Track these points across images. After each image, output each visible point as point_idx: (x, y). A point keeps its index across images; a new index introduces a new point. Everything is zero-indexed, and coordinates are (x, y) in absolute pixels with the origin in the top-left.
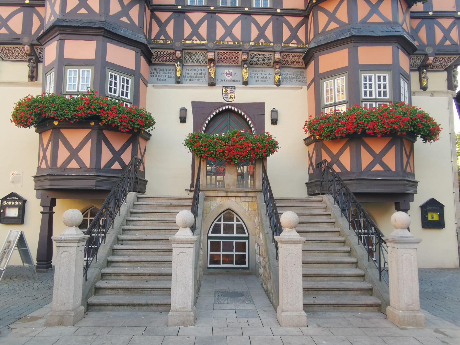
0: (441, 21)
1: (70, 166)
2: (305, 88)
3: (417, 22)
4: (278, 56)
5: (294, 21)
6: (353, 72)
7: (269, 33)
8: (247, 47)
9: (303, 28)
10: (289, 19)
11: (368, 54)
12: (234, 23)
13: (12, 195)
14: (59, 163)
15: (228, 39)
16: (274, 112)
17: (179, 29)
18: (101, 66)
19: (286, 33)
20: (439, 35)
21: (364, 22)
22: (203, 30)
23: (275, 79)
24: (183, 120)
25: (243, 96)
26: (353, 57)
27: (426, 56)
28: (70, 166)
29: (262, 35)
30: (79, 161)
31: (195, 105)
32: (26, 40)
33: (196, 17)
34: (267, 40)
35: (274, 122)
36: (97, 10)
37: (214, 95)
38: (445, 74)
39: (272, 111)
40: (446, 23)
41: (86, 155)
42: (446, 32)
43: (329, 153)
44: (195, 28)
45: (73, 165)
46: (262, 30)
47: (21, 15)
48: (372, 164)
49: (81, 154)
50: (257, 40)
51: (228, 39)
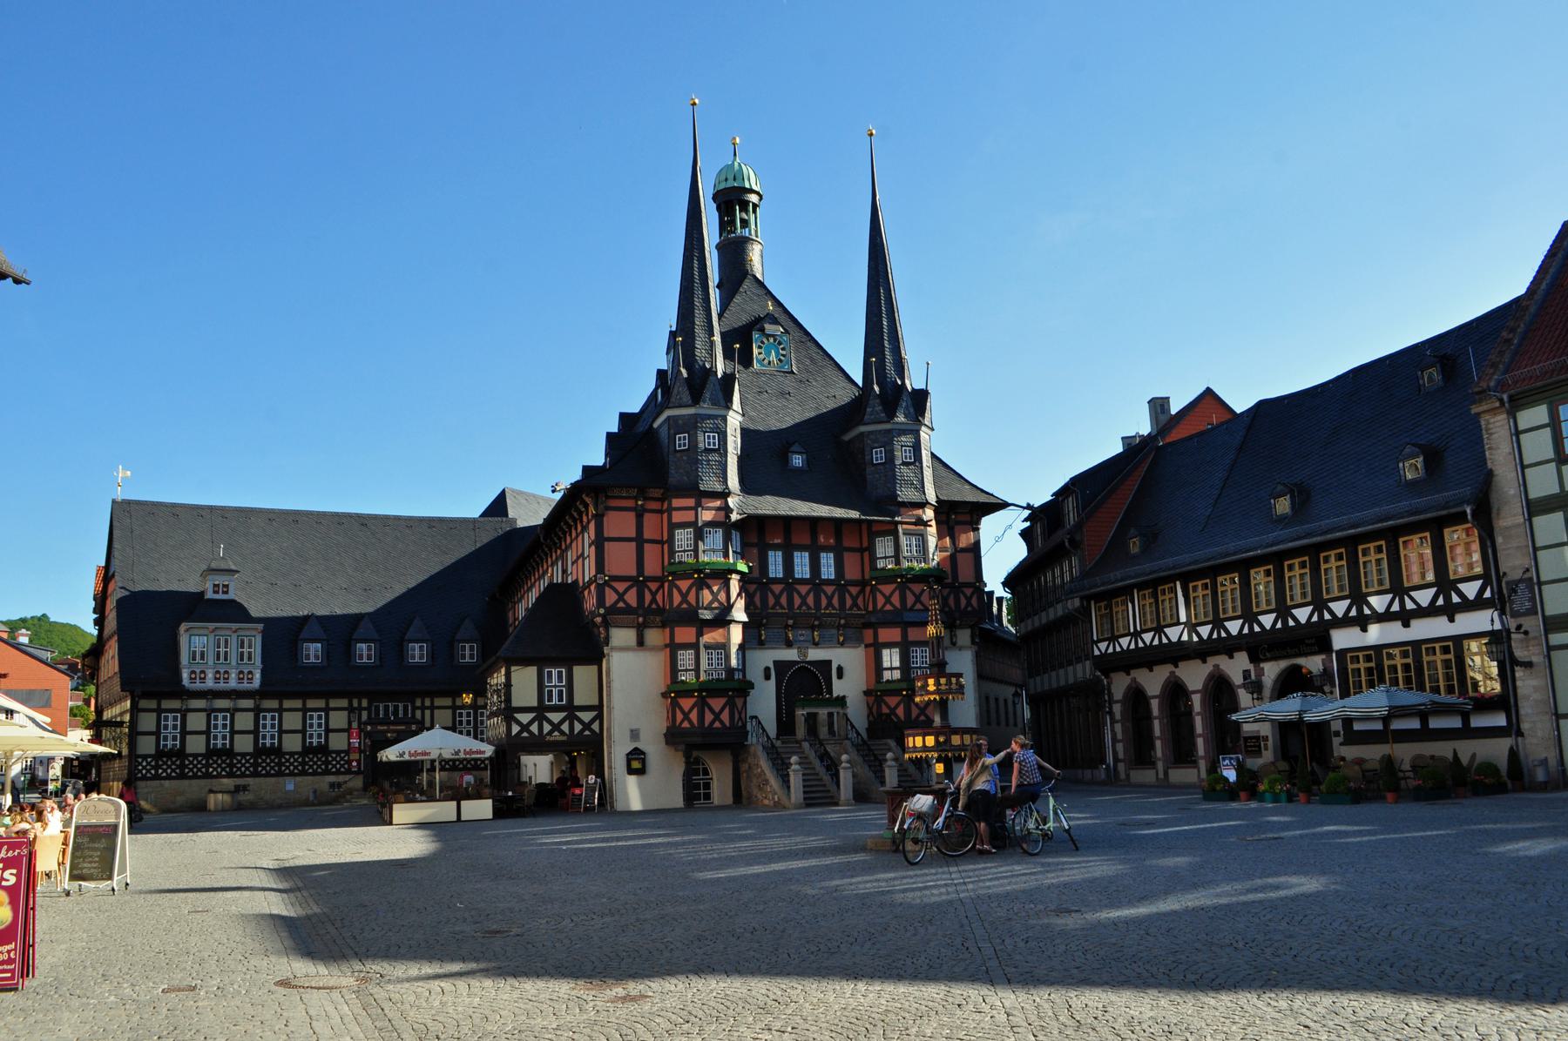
5: (854, 590)
6: (905, 648)
7: (835, 602)
12: (808, 593)
13: (636, 749)
16: (840, 670)
19: (849, 602)
20: (963, 602)
21: (911, 609)
22: (784, 600)
24: (767, 677)
25: (815, 654)
29: (830, 604)
30: (721, 722)
31: (776, 663)
33: (777, 588)
35: (840, 676)
37: (791, 655)
38: (968, 632)
40: (968, 592)
41: (725, 716)
42: (969, 599)
44: (777, 598)
45: (717, 724)
46: (830, 599)
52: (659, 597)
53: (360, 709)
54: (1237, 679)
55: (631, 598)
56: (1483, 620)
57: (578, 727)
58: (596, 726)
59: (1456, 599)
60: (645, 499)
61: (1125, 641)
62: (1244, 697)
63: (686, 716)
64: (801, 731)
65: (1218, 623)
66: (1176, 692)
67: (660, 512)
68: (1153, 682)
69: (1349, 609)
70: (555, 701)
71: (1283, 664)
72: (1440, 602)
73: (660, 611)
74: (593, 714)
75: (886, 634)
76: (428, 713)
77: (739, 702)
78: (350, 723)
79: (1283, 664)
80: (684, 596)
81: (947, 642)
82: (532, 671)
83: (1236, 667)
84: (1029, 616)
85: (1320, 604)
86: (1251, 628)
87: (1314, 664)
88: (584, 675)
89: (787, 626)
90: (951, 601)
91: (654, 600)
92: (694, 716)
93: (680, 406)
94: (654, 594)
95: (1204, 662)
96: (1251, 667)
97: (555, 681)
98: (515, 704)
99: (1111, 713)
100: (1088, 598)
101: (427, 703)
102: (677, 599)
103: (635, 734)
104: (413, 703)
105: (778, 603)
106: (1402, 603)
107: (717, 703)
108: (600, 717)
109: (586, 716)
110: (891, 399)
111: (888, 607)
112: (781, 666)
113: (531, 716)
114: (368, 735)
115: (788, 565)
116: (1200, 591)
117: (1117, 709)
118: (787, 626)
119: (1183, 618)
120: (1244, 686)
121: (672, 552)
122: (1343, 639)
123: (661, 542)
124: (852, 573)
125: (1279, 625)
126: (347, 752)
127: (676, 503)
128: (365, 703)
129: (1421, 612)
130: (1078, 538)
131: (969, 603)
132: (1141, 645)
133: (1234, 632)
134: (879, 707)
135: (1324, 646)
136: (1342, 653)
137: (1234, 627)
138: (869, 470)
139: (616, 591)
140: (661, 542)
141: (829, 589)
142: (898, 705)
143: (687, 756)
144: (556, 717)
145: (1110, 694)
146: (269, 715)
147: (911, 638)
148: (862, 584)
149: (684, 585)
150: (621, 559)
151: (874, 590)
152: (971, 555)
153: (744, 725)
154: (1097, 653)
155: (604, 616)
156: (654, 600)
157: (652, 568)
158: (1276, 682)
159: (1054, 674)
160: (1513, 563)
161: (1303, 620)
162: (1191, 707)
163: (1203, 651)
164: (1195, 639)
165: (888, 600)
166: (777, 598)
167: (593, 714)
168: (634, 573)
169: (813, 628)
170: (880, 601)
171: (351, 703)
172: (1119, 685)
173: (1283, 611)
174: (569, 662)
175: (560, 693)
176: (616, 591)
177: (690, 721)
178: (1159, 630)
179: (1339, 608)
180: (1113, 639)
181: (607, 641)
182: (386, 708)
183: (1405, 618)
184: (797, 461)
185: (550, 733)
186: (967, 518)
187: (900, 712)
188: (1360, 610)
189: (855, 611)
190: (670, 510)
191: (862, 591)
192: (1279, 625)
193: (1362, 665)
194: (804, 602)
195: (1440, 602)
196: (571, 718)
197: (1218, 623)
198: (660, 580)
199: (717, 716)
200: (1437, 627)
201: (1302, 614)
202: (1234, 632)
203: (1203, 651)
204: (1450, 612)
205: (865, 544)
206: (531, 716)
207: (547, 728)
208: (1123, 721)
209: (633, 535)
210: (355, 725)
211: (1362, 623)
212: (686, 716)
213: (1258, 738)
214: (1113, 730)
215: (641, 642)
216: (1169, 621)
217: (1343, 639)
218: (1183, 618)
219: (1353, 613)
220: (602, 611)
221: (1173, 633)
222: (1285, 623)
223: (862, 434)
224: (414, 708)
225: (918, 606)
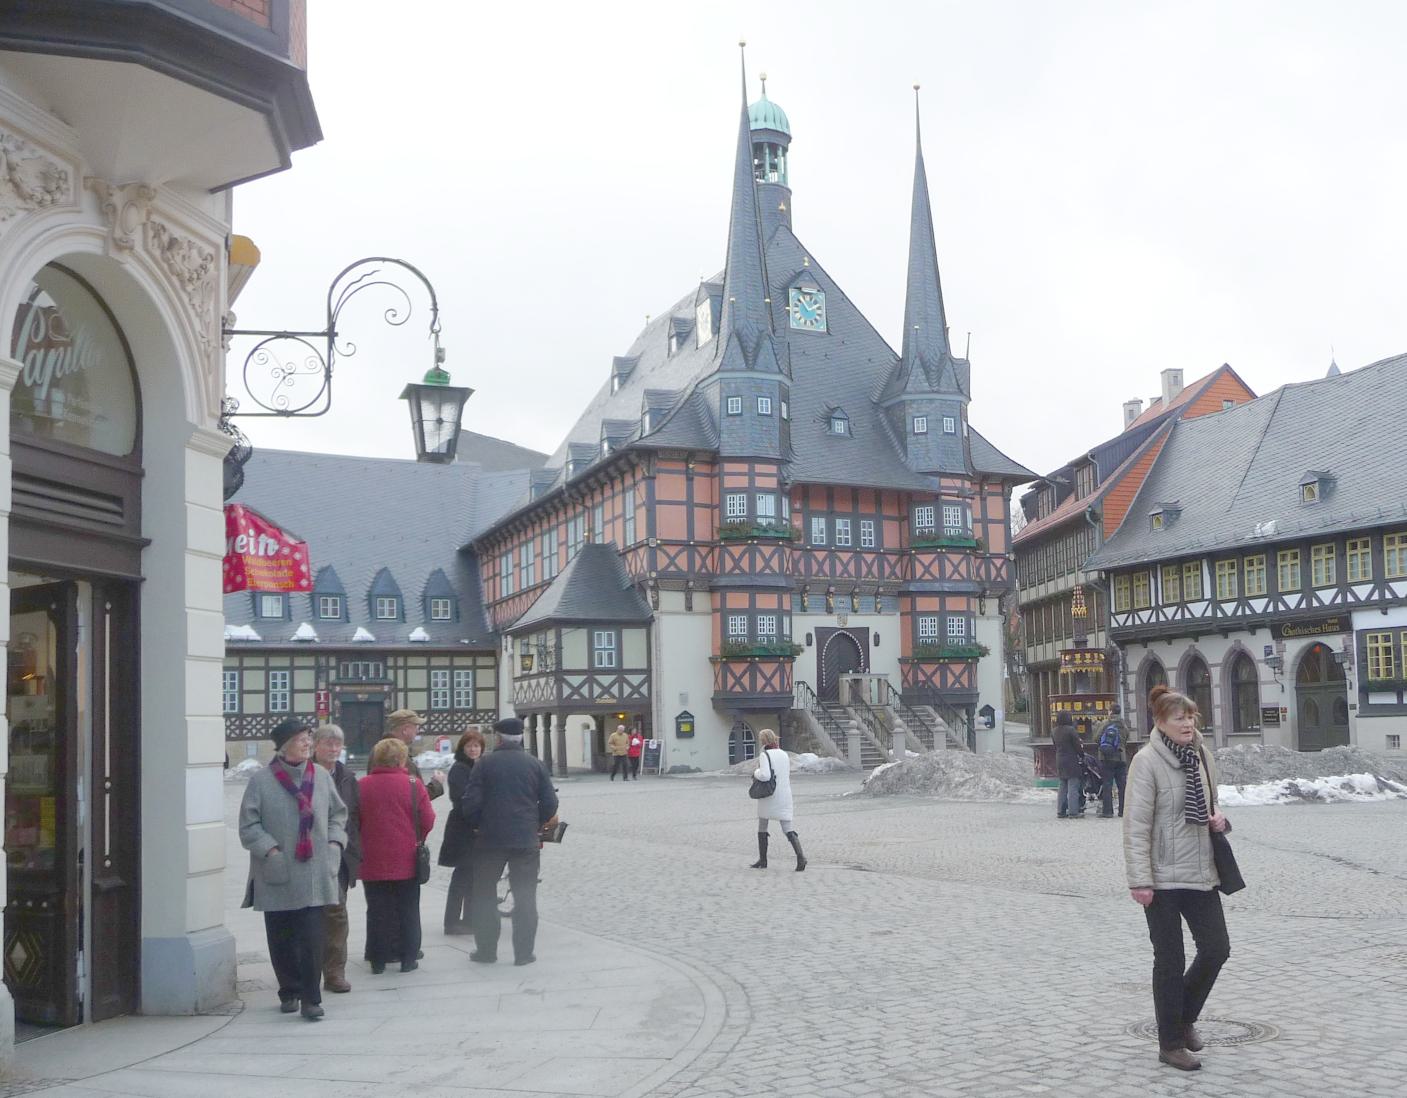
0: (994, 560)
1: (766, 691)
2: (899, 614)
3: (979, 561)
4: (881, 590)
5: (893, 559)
6: (942, 615)
7: (875, 569)
8: (859, 582)
9: (899, 565)
10: (889, 557)
11: (953, 604)
14: (759, 689)
15: (846, 575)
16: (877, 637)
17: (808, 566)
18: (780, 613)
19: (887, 571)
20: (994, 573)
23: (876, 607)
24: (809, 644)
25: (854, 622)
26: (942, 604)
27: (985, 590)
28: (766, 691)
29: (870, 572)
30: (772, 686)
32: (691, 576)
33: (820, 555)
34: (874, 577)
36: (778, 571)
37: (830, 621)
38: (997, 601)
39: (875, 636)
40: (998, 562)
41: (776, 681)
42: (999, 570)
43: (924, 674)
44: (821, 565)
45: (768, 689)
46: (870, 567)
47: (685, 553)
48: (954, 684)
49: (773, 682)
50: (866, 576)
51: (846, 575)
52: (709, 562)
53: (329, 668)
54: (1258, 654)
55: (682, 562)
57: (627, 690)
58: (644, 690)
60: (697, 462)
61: (1145, 615)
62: (1265, 672)
63: (738, 681)
64: (846, 695)
65: (1243, 600)
66: (1195, 665)
67: (711, 476)
68: (1171, 657)
69: (1371, 594)
70: (605, 664)
71: (1304, 642)
73: (711, 575)
74: (643, 677)
75: (923, 604)
76: (401, 673)
77: (787, 667)
78: (317, 683)
79: (1304, 642)
80: (737, 562)
81: (978, 613)
82: (582, 633)
83: (1257, 644)
84: (1033, 585)
85: (1344, 587)
86: (1276, 607)
87: (1335, 643)
88: (633, 639)
89: (828, 593)
90: (982, 571)
91: (704, 565)
92: (746, 680)
93: (733, 370)
94: (704, 559)
95: (1226, 637)
96: (1273, 643)
97: (605, 644)
98: (566, 666)
99: (1124, 683)
100: (1108, 571)
101: (401, 662)
102: (729, 564)
103: (684, 698)
104: (385, 663)
105: (821, 569)
107: (768, 669)
108: (648, 680)
109: (635, 680)
110: (933, 365)
111: (927, 577)
112: (822, 633)
114: (336, 696)
115: (831, 529)
116: (1225, 571)
117: (1132, 680)
118: (828, 593)
119: (1208, 595)
120: (1267, 662)
121: (723, 516)
122: (1362, 621)
123: (712, 507)
124: (892, 538)
125: (1303, 605)
126: (314, 715)
127: (728, 467)
128: (333, 662)
130: (1098, 511)
131: (999, 574)
132: (1162, 618)
133: (1259, 610)
134: (915, 676)
135: (1345, 626)
136: (1362, 633)
137: (1259, 605)
138: (910, 439)
139: (668, 555)
140: (712, 507)
141: (869, 558)
142: (934, 673)
143: (740, 725)
144: (606, 680)
145: (1125, 665)
146: (279, 674)
147: (948, 608)
148: (902, 553)
149: (737, 551)
150: (672, 523)
151: (911, 561)
152: (1000, 528)
153: (791, 692)
154: (1114, 624)
155: (655, 580)
156: (704, 565)
157: (702, 532)
158: (1297, 657)
159: (1040, 647)
161: (1327, 603)
162: (1209, 678)
163: (1225, 628)
164: (1220, 615)
165: (927, 569)
166: (821, 565)
167: (643, 677)
168: (684, 537)
169: (852, 595)
170: (919, 570)
171: (317, 662)
172: (1135, 658)
173: (1308, 591)
174: (618, 625)
175: (610, 655)
176: (668, 555)
177: (742, 685)
178: (1182, 605)
179: (1362, 591)
180: (1133, 612)
181: (656, 604)
182: (356, 668)
184: (839, 427)
185: (600, 696)
186: (999, 489)
187: (937, 679)
188: (1382, 594)
189: (893, 580)
190: (720, 475)
191: (900, 560)
192: (1303, 605)
193: (1381, 644)
194: (845, 570)
196: (621, 681)
197: (1243, 600)
198: (711, 546)
199: (768, 681)
201: (1327, 596)
202: (1259, 610)
203: (1225, 628)
205: (906, 514)
207: (597, 691)
208: (1138, 691)
209: (684, 499)
210: (322, 685)
211: (1384, 606)
212: (738, 681)
213: (1277, 709)
214: (1126, 701)
215: (689, 608)
216: (1193, 598)
218: (1208, 595)
219: (1376, 597)
220: (654, 575)
221: (1197, 610)
222: (1309, 603)
223: (903, 402)
224: (386, 668)
225: (956, 576)
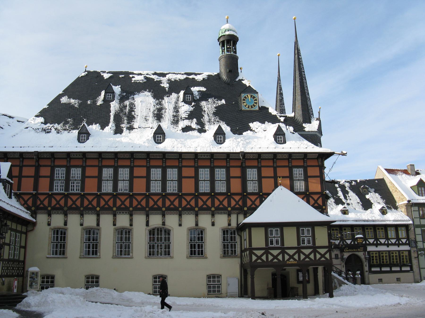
56: (407, 248)
59: (401, 242)
69: (374, 241)
72: (397, 242)
79: (350, 253)
106: (388, 242)
113: (295, 251)
125: (353, 243)
129: (392, 244)
135: (365, 250)
160: (412, 236)
183: (388, 245)
192: (353, 243)
195: (397, 242)
200: (395, 248)
204: (399, 245)
206: (295, 251)
217: (370, 248)
